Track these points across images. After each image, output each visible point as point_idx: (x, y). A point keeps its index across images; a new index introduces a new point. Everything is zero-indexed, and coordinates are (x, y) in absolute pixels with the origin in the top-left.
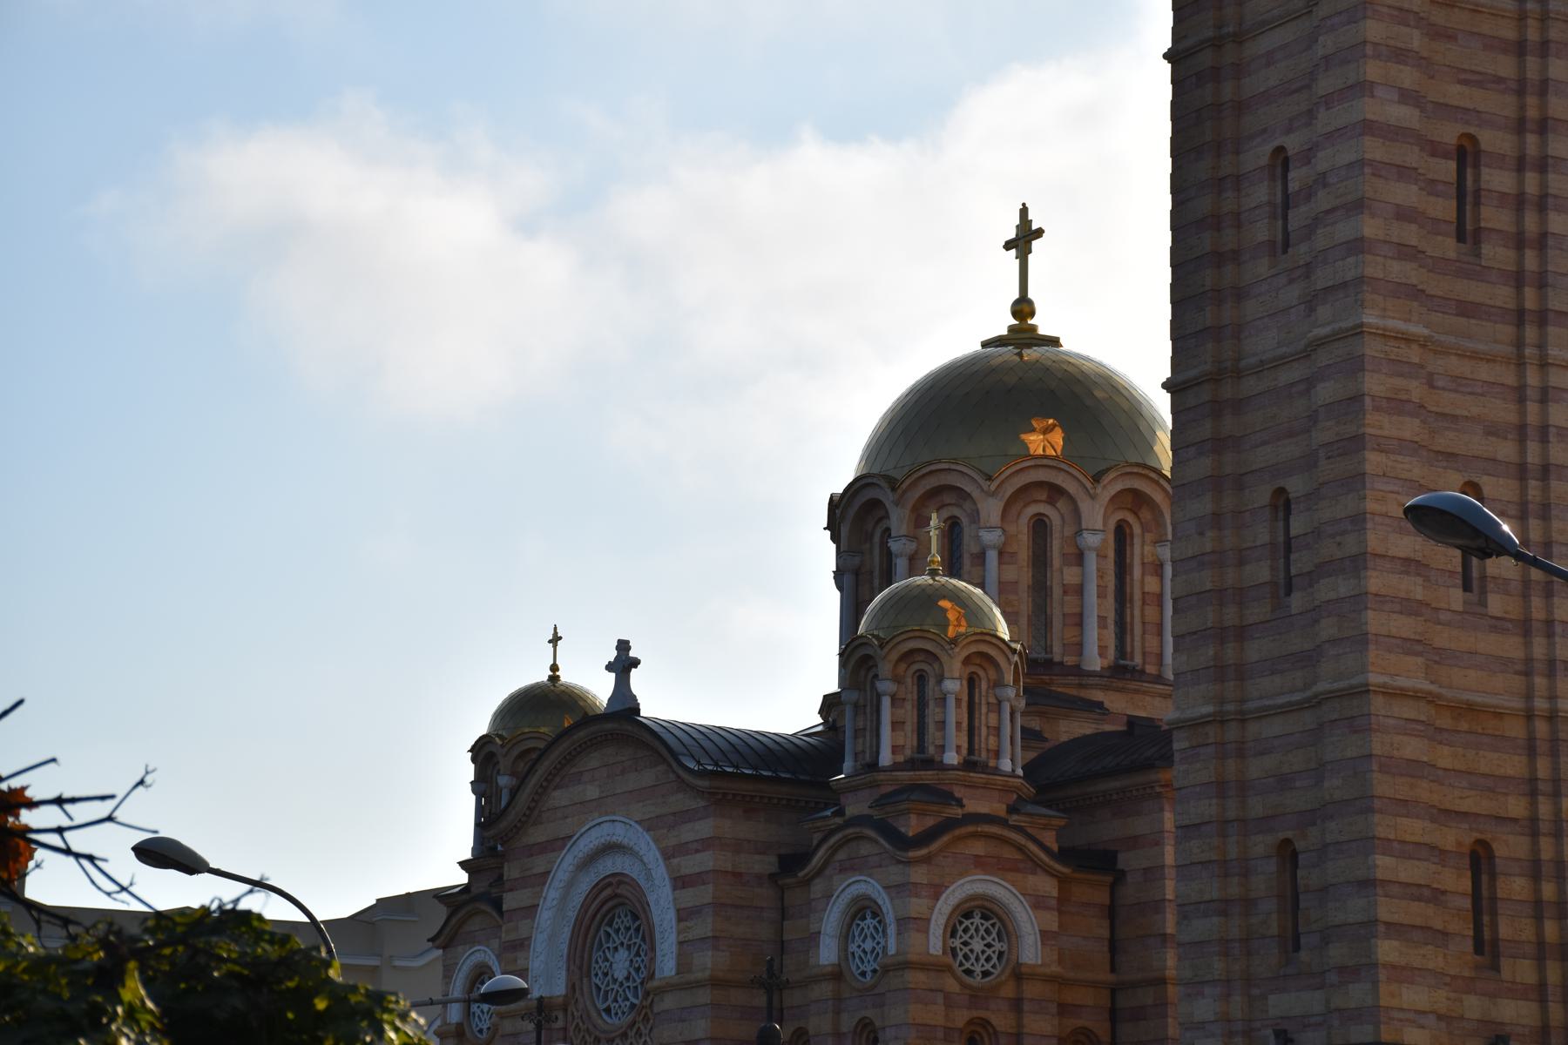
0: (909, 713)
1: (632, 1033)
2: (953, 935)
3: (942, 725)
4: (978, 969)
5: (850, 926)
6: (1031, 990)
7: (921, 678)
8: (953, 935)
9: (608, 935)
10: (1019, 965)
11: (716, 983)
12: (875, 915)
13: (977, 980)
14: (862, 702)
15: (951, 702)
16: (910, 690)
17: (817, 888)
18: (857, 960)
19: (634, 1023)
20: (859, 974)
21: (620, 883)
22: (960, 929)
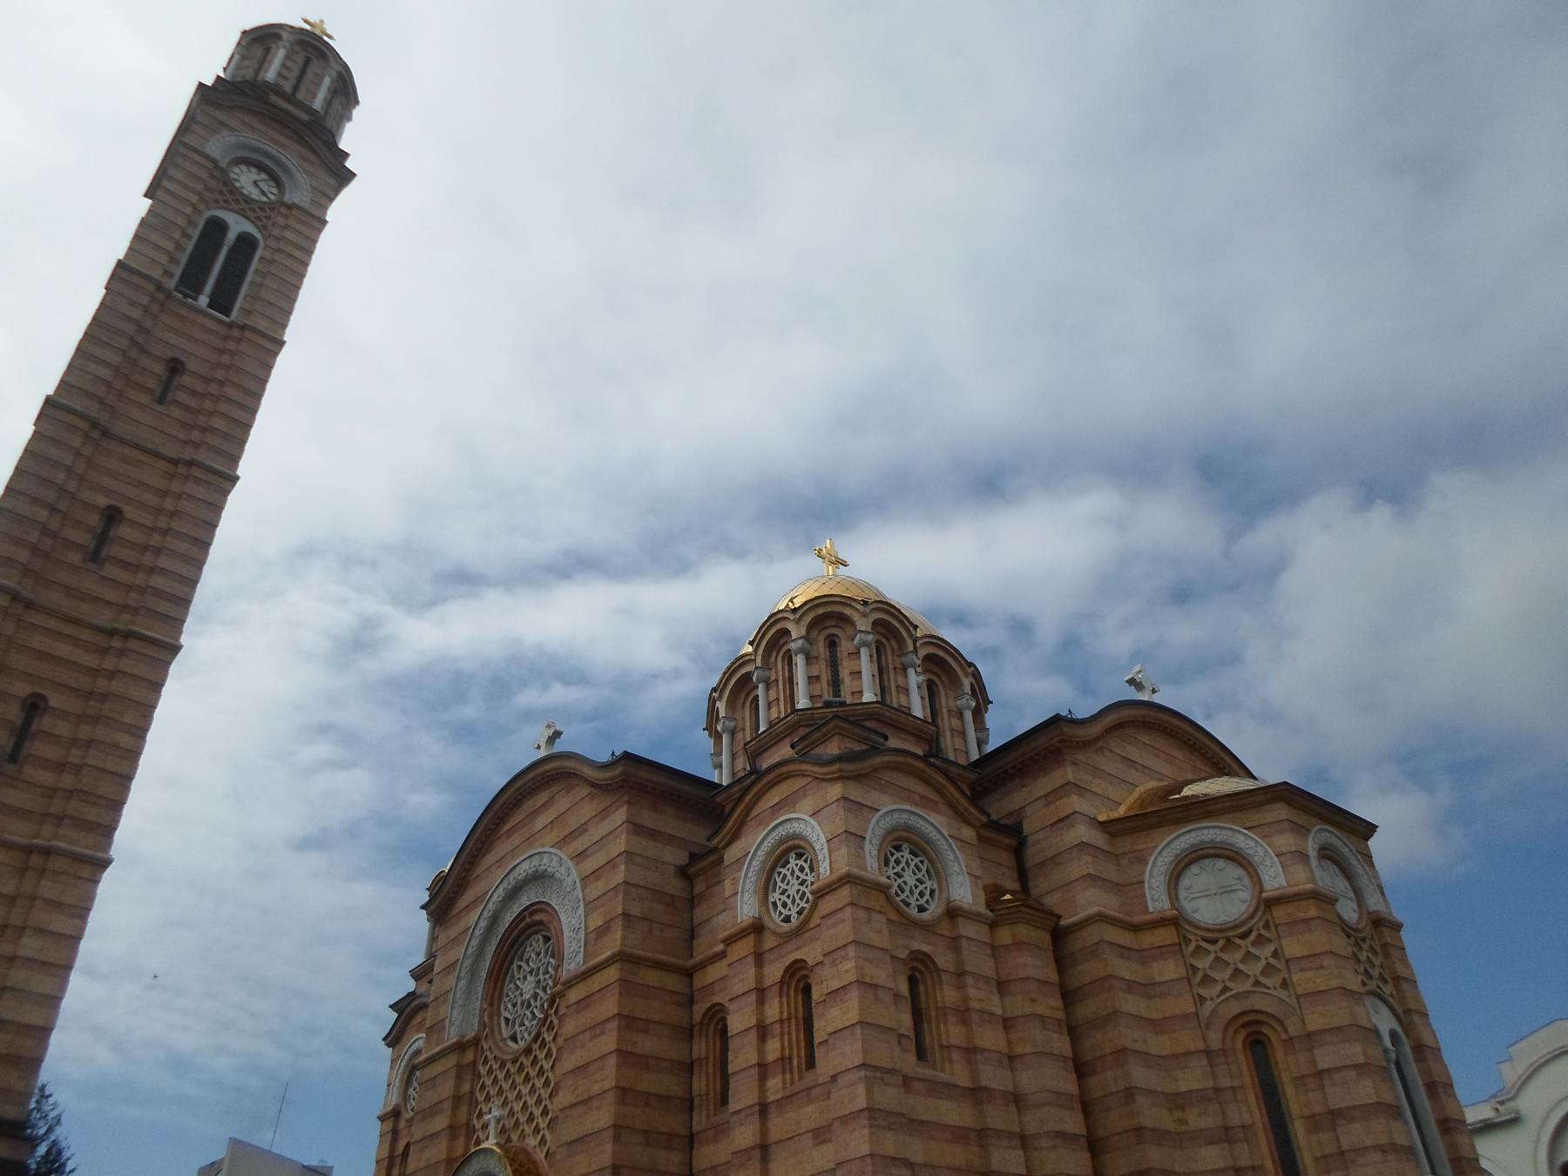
0: (822, 669)
1: (535, 1046)
2: (887, 863)
3: (857, 674)
4: (913, 901)
5: (772, 869)
6: (968, 929)
7: (832, 644)
8: (887, 863)
9: (520, 967)
10: (949, 902)
11: (621, 957)
12: (799, 856)
13: (913, 912)
14: (773, 678)
15: (864, 652)
16: (821, 649)
17: (731, 854)
18: (780, 908)
19: (538, 1034)
20: (782, 921)
21: (531, 914)
22: (892, 860)
